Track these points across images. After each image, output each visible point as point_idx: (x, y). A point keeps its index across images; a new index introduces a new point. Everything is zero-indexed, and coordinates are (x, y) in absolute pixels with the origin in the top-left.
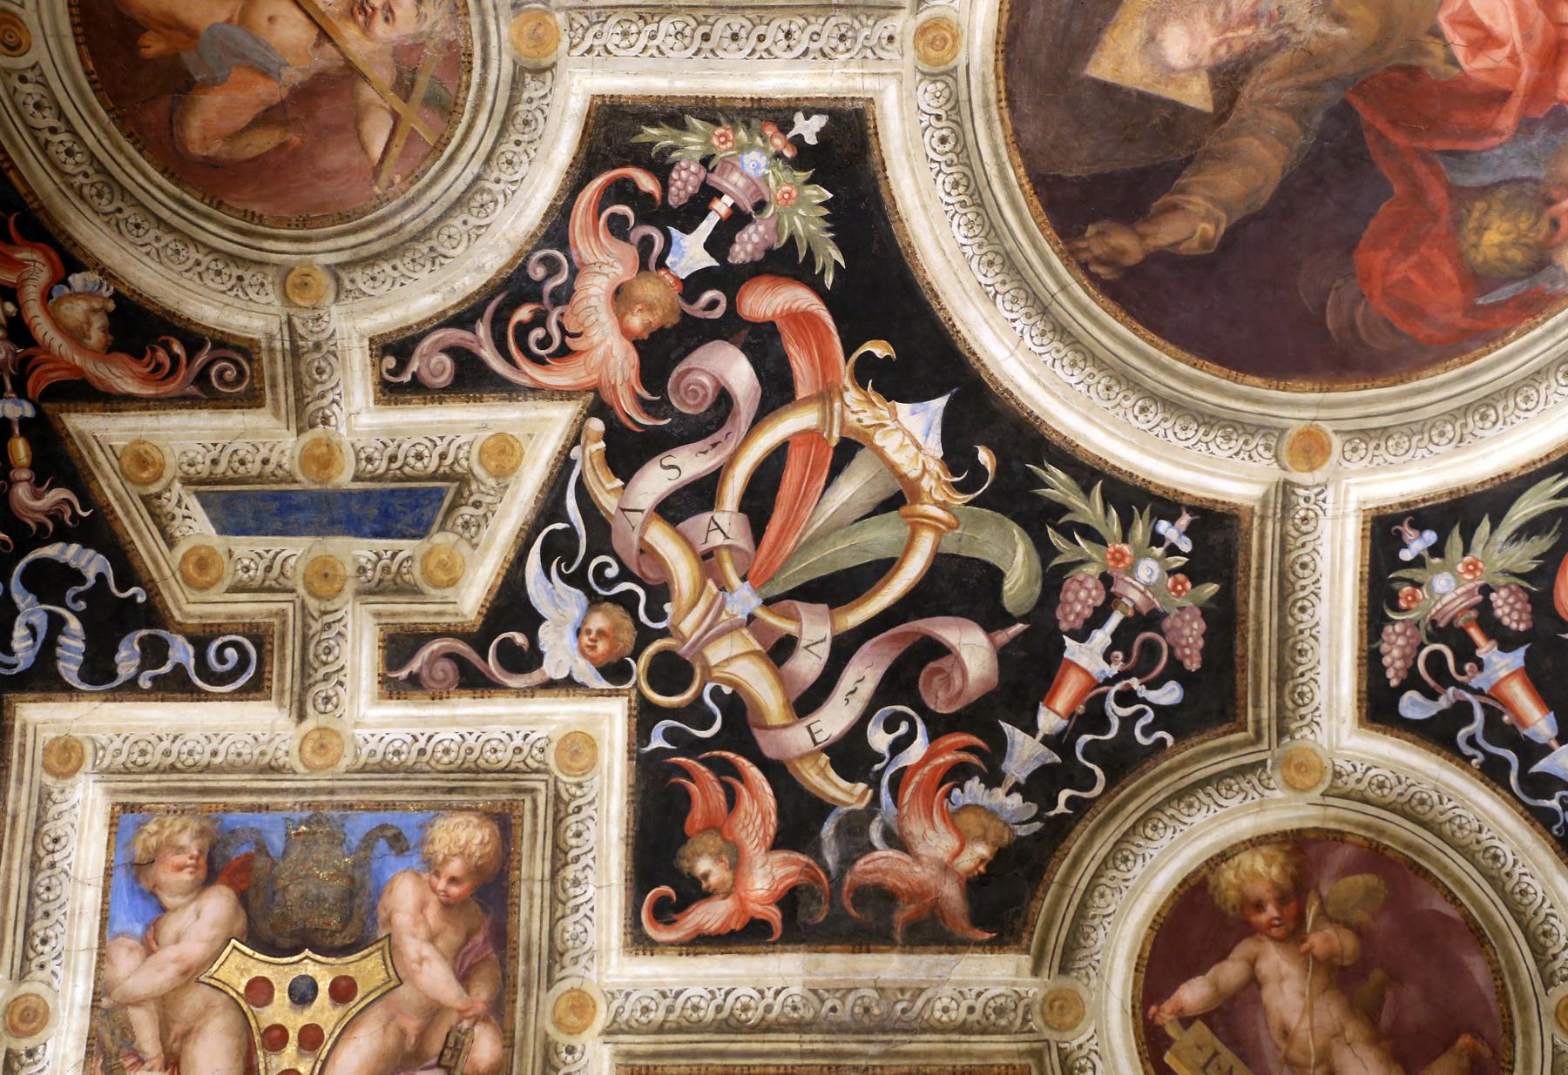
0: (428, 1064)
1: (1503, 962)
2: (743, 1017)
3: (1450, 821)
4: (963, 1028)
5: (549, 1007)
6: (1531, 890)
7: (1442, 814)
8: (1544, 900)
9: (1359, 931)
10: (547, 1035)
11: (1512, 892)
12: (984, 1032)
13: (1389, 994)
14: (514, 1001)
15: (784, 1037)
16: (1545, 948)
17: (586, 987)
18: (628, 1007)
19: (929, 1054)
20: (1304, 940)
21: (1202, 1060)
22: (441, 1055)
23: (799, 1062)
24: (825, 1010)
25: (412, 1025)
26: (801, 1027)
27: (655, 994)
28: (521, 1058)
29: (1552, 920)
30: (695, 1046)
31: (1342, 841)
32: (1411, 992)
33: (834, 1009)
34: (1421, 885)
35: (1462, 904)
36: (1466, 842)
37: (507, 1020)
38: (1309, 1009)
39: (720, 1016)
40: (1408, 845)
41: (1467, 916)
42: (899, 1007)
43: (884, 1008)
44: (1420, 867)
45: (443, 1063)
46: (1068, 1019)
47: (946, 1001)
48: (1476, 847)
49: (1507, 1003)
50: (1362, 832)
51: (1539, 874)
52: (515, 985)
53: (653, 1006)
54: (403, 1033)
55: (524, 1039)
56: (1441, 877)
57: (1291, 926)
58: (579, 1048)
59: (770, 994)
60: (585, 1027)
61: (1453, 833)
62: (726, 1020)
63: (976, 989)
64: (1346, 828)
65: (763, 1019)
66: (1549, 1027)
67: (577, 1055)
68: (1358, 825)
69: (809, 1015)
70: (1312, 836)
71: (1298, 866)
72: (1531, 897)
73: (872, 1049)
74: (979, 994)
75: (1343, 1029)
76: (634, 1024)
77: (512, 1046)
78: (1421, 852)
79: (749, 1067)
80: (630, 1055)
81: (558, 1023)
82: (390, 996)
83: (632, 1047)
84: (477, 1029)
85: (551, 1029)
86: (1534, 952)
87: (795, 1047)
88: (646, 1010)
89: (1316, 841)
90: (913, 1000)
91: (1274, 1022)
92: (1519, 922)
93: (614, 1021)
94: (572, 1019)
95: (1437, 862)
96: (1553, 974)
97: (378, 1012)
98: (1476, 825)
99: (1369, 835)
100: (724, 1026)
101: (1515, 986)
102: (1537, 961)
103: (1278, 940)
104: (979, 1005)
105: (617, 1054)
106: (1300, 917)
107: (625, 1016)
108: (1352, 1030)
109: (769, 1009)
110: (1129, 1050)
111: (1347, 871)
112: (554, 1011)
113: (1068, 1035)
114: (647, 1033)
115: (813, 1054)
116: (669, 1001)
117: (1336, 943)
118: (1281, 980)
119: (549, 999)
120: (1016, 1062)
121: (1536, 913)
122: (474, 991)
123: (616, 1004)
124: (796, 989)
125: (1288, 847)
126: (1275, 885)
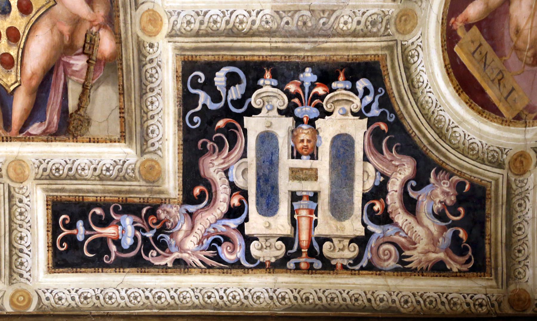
0: (78, 52)
2: (240, 27)
4: (354, 34)
5: (138, 20)
10: (138, 37)
12: (365, 36)
14: (119, 16)
15: (261, 39)
17: (156, 9)
18: (179, 21)
19: (336, 49)
21: (473, 49)
22: (84, 47)
23: (270, 54)
24: (283, 23)
25: (66, 29)
26: (270, 33)
27: (193, 14)
28: (126, 50)
30: (216, 44)
33: (287, 23)
37: (116, 27)
39: (228, 27)
42: (322, 21)
43: (314, 22)
45: (85, 51)
46: (408, 27)
47: (346, 17)
52: (118, 7)
53: (192, 20)
54: (61, 34)
55: (126, 38)
58: (156, 44)
59: (254, 14)
60: (158, 32)
62: (231, 29)
63: (363, 10)
65: (251, 29)
67: (155, 49)
69: (275, 26)
73: (307, 46)
74: (364, 13)
76: (183, 31)
77: (120, 42)
79: (244, 56)
80: (182, 49)
81: (143, 30)
82: (51, 11)
83: (183, 44)
84: (102, 32)
85: (140, 34)
87: (267, 45)
88: (189, 23)
90: (329, 18)
93: (173, 29)
94: (150, 28)
97: (45, 22)
100: (230, 33)
104: (363, 20)
105: (176, 48)
107: (178, 26)
109: (253, 23)
110: (437, 45)
112: (140, 23)
113: (407, 37)
114: (191, 36)
115: (277, 49)
116: (201, 18)
119: (137, 14)
120: (380, 53)
122: (96, 10)
123: (173, 19)
124: (268, 11)
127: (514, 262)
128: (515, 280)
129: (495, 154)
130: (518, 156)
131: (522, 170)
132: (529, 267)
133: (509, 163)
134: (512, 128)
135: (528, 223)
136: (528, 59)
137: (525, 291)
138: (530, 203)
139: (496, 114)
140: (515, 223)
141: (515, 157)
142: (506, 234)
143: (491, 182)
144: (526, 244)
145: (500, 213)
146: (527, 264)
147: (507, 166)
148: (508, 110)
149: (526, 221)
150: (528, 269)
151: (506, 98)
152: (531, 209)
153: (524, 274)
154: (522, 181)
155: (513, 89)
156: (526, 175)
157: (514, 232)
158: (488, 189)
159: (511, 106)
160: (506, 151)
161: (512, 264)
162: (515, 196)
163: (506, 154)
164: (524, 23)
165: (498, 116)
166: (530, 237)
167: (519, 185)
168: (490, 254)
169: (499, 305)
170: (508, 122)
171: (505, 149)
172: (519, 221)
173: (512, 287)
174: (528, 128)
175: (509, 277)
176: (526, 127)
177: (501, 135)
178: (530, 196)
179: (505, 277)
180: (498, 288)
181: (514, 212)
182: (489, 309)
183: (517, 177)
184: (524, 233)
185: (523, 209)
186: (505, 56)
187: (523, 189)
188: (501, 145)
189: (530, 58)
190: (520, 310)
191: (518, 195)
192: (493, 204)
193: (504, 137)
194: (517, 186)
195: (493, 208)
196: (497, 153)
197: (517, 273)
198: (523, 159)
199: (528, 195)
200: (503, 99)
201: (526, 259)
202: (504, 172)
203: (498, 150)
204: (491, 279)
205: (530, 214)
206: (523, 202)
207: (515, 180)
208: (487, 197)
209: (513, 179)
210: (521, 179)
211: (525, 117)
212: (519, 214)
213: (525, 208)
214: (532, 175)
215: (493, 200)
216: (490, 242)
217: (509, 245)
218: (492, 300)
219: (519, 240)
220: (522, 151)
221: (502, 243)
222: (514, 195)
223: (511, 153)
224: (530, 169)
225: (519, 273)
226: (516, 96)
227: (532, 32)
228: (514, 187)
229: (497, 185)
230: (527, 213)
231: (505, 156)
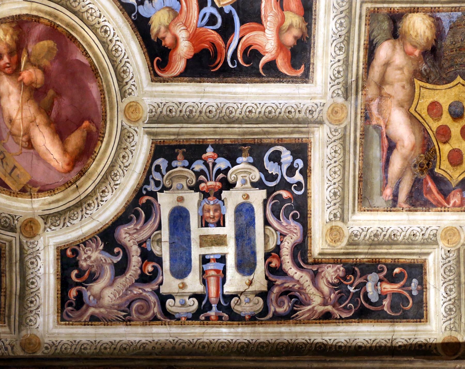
1: (105, 86)
3: (87, 11)
6: (120, 49)
7: (83, 7)
8: (125, 54)
9: (45, 71)
11: (112, 51)
13: (56, 102)
16: (123, 79)
20: (20, 75)
29: (128, 65)
31: (39, 21)
32: (65, 101)
34: (73, 46)
35: (90, 57)
36: (93, 23)
38: (21, 109)
40: (68, 25)
41: (92, 62)
44: (73, 37)
48: (97, 26)
49: (105, 106)
50: (47, 17)
51: (124, 40)
56: (81, 42)
57: (14, 67)
61: (88, 18)
64: (41, 15)
66: (121, 116)
68: (46, 13)
70: (25, 19)
71: (18, 36)
72: (119, 53)
75: (35, 119)
78: (73, 28)
86: (118, 80)
89: (27, 22)
91: (6, 115)
92: (113, 66)
95: (80, 34)
96: (125, 92)
98: (98, 13)
99: (51, 19)
101: (109, 98)
102: (119, 85)
103: (8, 74)
106: (19, 62)
108: (40, 119)
111: (40, 39)
117: (34, 77)
118: (9, 94)
121: (121, 61)
125: (14, 25)
126: (8, 46)
127: (26, 311)
128: (26, 326)
129: (7, 220)
130: (28, 222)
131: (32, 233)
132: (40, 315)
133: (20, 227)
134: (20, 199)
135: (40, 278)
136: (24, 144)
137: (35, 336)
138: (41, 261)
139: (4, 187)
140: (28, 278)
141: (25, 223)
142: (20, 287)
143: (5, 244)
144: (38, 296)
145: (14, 269)
146: (38, 313)
147: (18, 230)
148: (13, 184)
149: (38, 277)
150: (39, 317)
151: (10, 174)
152: (42, 267)
153: (35, 322)
154: (33, 243)
155: (15, 167)
156: (37, 238)
157: (28, 286)
158: (3, 249)
159: (15, 181)
160: (17, 217)
161: (24, 313)
162: (28, 255)
163: (17, 220)
164: (15, 114)
165: (5, 189)
166: (42, 290)
167: (30, 246)
168: (5, 304)
169: (12, 348)
170: (16, 194)
171: (16, 216)
172: (32, 276)
173: (24, 333)
174: (33, 199)
175: (20, 324)
176: (31, 198)
177: (10, 204)
178: (41, 256)
179: (17, 323)
180: (11, 334)
181: (27, 269)
182: (3, 352)
183: (28, 239)
184: (36, 286)
185: (35, 266)
186: (4, 140)
187: (34, 250)
188: (12, 212)
189: (25, 142)
190: (31, 352)
191: (30, 254)
192: (7, 262)
193: (13, 206)
194: (28, 247)
195: (7, 265)
196: (9, 219)
197: (28, 321)
198: (32, 225)
199: (39, 255)
200: (7, 175)
201: (38, 308)
202: (17, 235)
203: (9, 216)
204: (5, 326)
205: (42, 271)
206: (34, 260)
207: (27, 242)
208: (2, 256)
209: (25, 241)
210: (32, 241)
211: (29, 190)
212: (31, 271)
213: (37, 266)
214: (42, 238)
215: (8, 258)
216: (6, 294)
217: (22, 297)
218: (5, 344)
219: (32, 293)
220: (31, 218)
221: (16, 295)
222: (26, 255)
223: (22, 220)
224: (40, 233)
225: (31, 320)
226: (18, 172)
227: (24, 121)
228: (26, 247)
229: (11, 247)
230: (39, 270)
231: (16, 222)
